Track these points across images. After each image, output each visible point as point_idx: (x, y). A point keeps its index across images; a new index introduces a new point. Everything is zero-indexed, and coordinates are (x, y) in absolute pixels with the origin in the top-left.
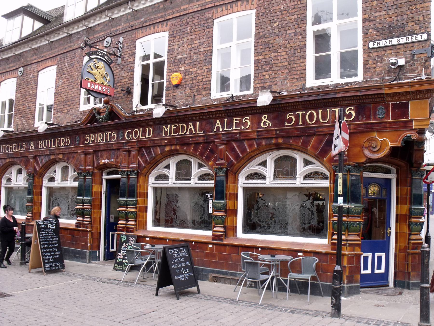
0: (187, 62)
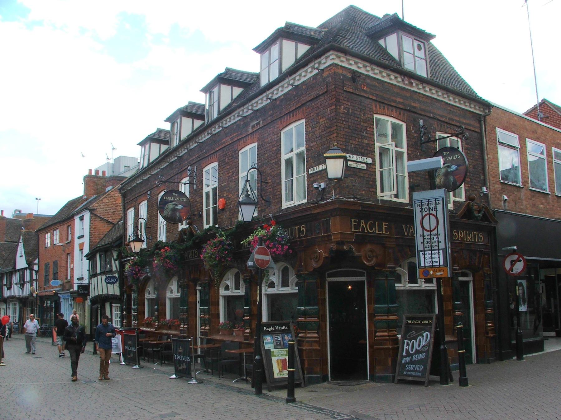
0: (227, 189)
